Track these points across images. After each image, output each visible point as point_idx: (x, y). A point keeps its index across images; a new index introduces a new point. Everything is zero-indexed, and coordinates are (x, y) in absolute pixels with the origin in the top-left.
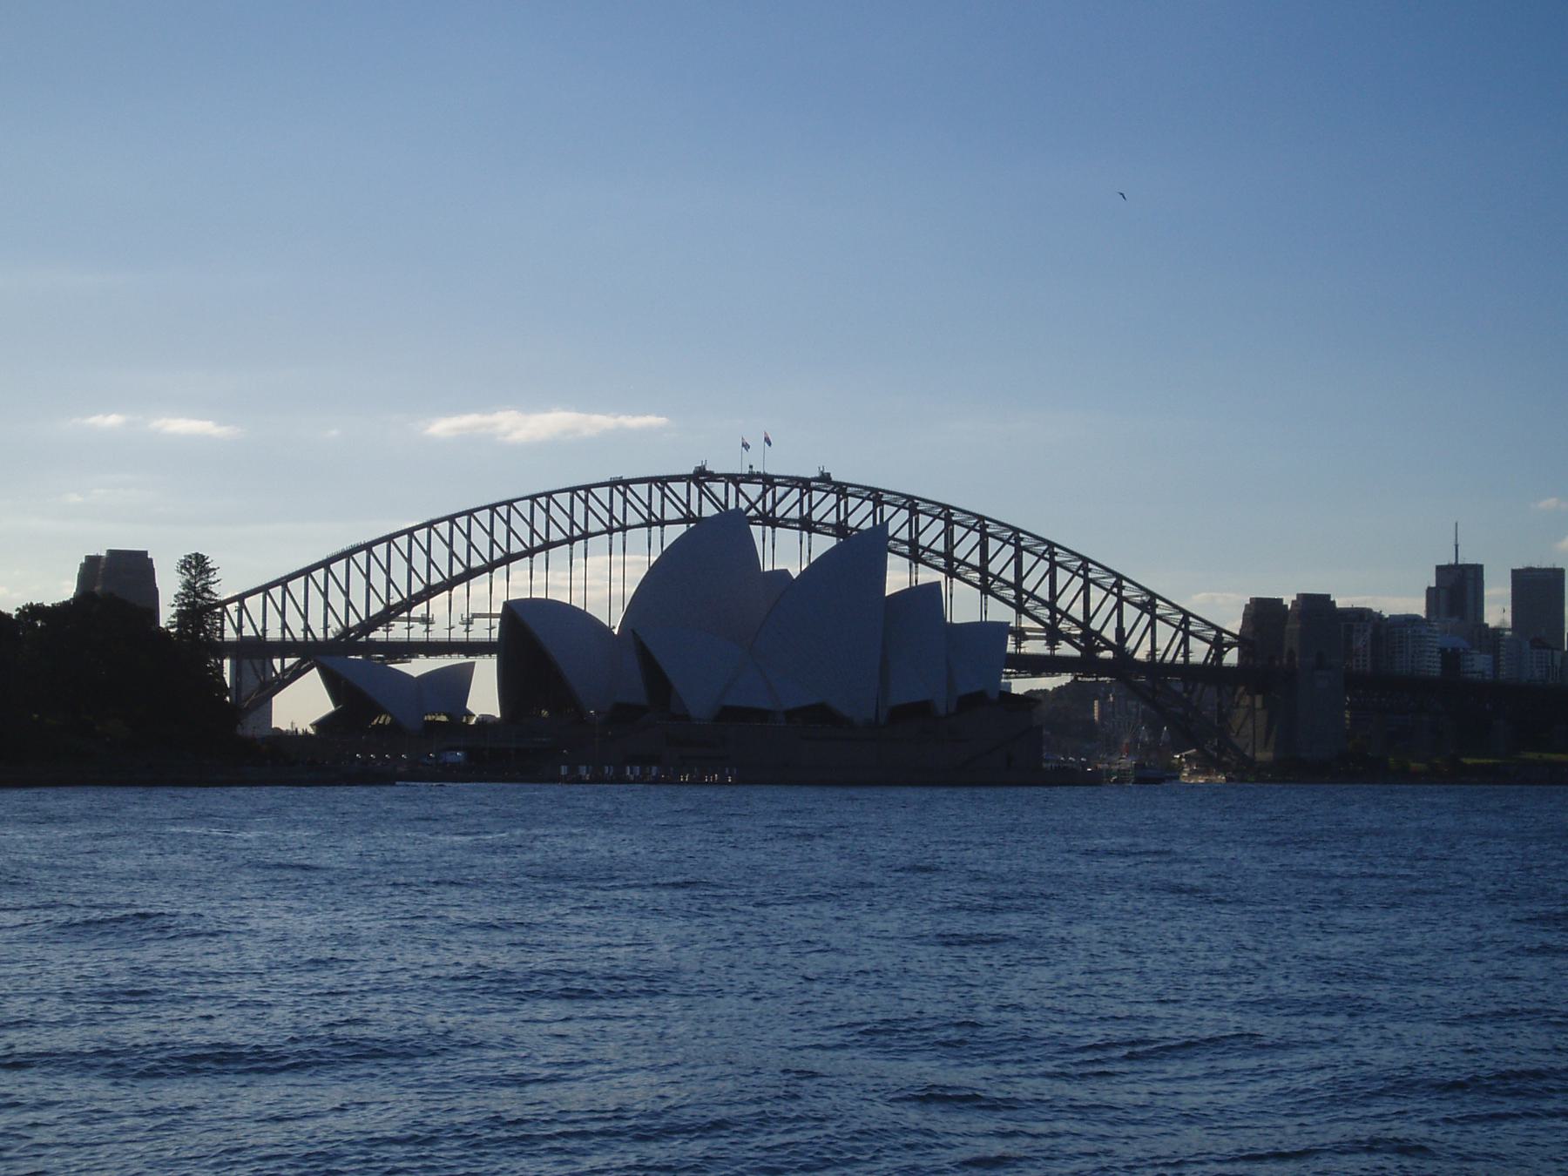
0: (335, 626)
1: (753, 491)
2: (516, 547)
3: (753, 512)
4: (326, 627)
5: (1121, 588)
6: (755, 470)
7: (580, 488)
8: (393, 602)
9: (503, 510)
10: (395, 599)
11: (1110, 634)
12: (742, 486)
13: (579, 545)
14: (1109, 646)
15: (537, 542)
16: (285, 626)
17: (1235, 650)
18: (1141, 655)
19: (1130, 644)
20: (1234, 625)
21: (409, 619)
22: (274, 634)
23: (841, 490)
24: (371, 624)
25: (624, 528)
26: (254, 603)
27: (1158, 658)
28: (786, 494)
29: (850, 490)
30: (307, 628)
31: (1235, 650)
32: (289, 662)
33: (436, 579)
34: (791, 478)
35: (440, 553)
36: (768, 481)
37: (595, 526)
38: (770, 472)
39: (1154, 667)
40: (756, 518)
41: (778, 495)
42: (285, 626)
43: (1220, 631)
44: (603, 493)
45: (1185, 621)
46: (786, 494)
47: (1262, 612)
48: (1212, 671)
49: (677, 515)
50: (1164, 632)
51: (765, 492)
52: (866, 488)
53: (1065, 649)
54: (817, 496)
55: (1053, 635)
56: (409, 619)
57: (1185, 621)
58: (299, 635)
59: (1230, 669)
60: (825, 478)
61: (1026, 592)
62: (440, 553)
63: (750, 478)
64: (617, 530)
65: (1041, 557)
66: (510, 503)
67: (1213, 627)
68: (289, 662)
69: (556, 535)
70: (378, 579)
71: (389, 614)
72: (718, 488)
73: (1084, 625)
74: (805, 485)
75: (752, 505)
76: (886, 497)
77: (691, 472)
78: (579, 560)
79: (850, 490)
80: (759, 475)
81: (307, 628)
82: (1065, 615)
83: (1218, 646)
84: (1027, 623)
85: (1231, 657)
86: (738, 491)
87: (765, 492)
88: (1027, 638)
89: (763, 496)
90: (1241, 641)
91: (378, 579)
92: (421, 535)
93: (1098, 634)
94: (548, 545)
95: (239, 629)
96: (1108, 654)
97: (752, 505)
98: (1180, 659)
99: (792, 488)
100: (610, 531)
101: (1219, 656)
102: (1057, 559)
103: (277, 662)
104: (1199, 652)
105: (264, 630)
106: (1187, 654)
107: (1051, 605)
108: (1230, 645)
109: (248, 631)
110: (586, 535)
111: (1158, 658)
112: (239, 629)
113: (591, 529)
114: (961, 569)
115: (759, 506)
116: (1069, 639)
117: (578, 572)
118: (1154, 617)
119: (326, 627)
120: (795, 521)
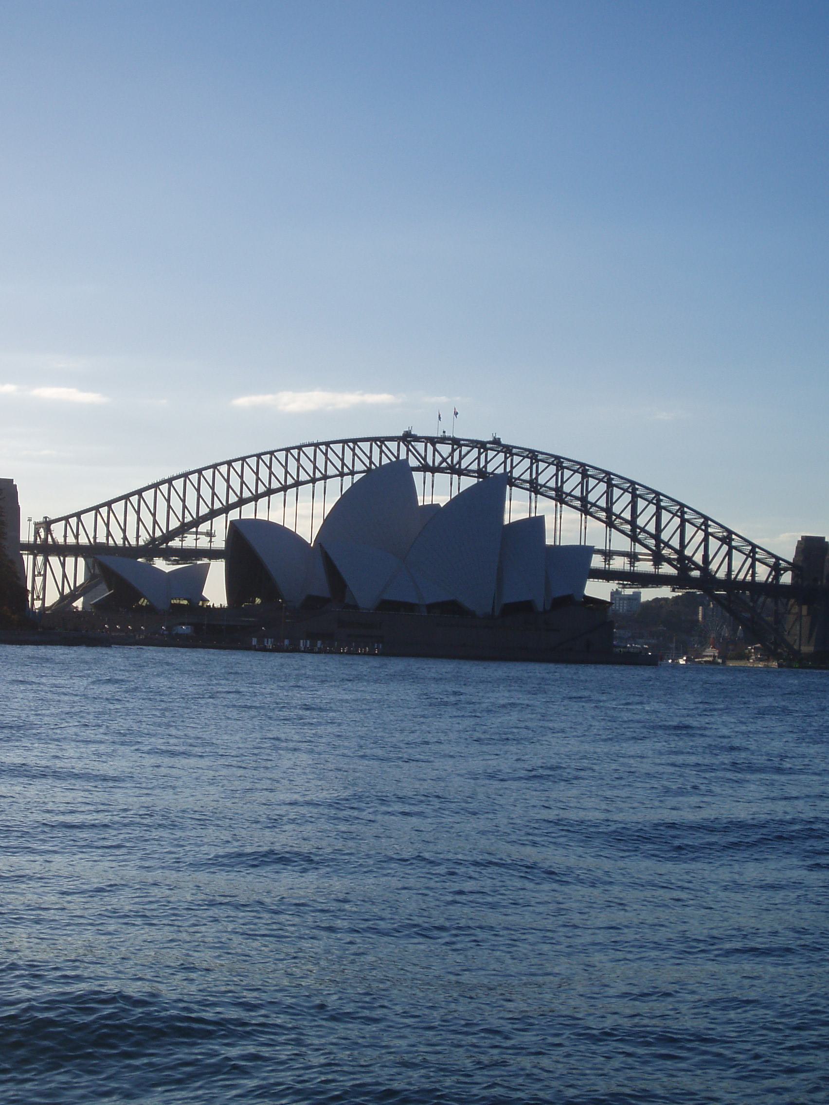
0: (144, 538)
1: (445, 449)
2: (275, 485)
3: (444, 465)
4: (138, 537)
5: (707, 526)
6: (447, 434)
7: (322, 444)
8: (186, 521)
10: (188, 519)
11: (698, 558)
12: (438, 446)
13: (320, 484)
14: (697, 567)
15: (290, 481)
16: (109, 534)
17: (789, 573)
18: (721, 575)
19: (713, 567)
20: (788, 553)
23: (508, 450)
24: (170, 535)
26: (88, 519)
27: (733, 577)
28: (469, 452)
29: (514, 451)
30: (125, 538)
31: (789, 573)
33: (217, 505)
34: (472, 441)
35: (221, 487)
36: (456, 442)
37: (331, 471)
38: (457, 436)
39: (729, 583)
40: (446, 468)
41: (463, 453)
42: (109, 534)
43: (778, 559)
44: (338, 448)
45: (753, 551)
46: (469, 452)
47: (811, 547)
48: (772, 589)
50: (738, 559)
51: (453, 450)
52: (526, 450)
53: (666, 569)
54: (491, 454)
55: (658, 558)
56: (197, 533)
57: (753, 551)
58: (120, 542)
59: (785, 586)
60: (496, 442)
61: (639, 528)
62: (221, 487)
63: (443, 440)
64: (347, 474)
65: (650, 502)
66: (271, 453)
67: (773, 556)
69: (303, 477)
71: (183, 529)
72: (420, 447)
73: (680, 552)
74: (481, 446)
75: (444, 460)
76: (540, 457)
77: (401, 434)
79: (514, 451)
80: (449, 439)
81: (125, 538)
82: (667, 545)
83: (776, 569)
84: (639, 549)
85: (786, 578)
86: (435, 450)
87: (453, 450)
88: (639, 560)
89: (451, 455)
90: (793, 567)
93: (690, 559)
94: (298, 484)
95: (77, 537)
96: (696, 573)
97: (444, 460)
98: (749, 578)
99: (473, 448)
101: (777, 577)
102: (662, 504)
104: (763, 573)
105: (95, 538)
106: (753, 575)
107: (657, 537)
108: (786, 570)
109: (83, 540)
110: (325, 477)
111: (733, 577)
112: (77, 537)
113: (329, 473)
114: (593, 509)
115: (449, 460)
116: (669, 561)
118: (731, 548)
119: (138, 537)
120: (474, 471)
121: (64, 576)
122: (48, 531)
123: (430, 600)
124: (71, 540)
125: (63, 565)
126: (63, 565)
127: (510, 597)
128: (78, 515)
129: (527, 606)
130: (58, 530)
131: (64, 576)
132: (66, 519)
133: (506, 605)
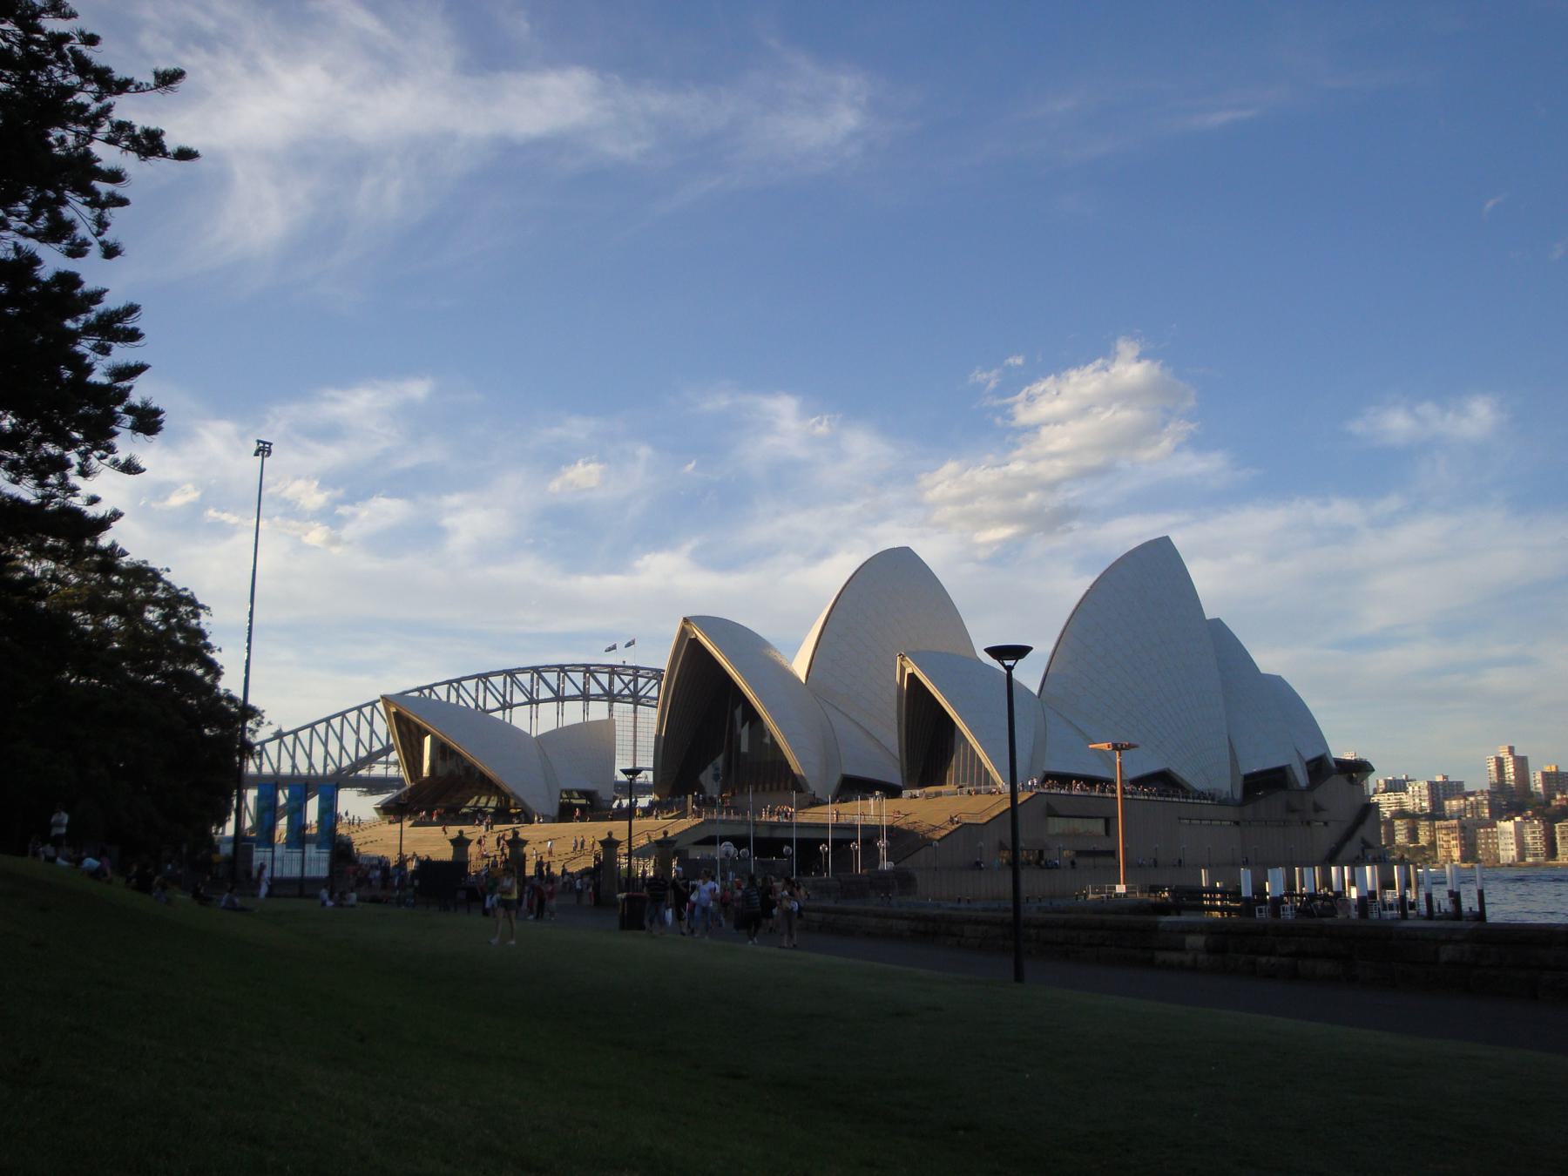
0: (331, 768)
16: (294, 766)
21: (387, 762)
22: (286, 769)
24: (359, 763)
25: (511, 706)
30: (311, 765)
42: (294, 766)
49: (550, 695)
56: (387, 762)
70: (334, 748)
71: (372, 758)
81: (311, 765)
91: (334, 748)
113: (489, 707)
119: (325, 766)
127: (1255, 764)
133: (1247, 777)
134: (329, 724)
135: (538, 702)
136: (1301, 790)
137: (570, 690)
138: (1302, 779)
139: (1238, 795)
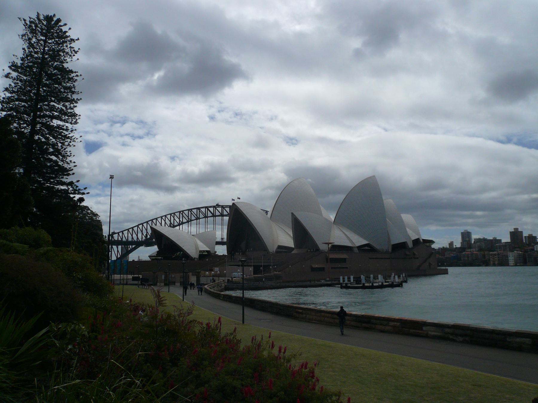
9: (173, 215)
13: (181, 226)
16: (132, 238)
22: (130, 239)
25: (199, 219)
26: (126, 233)
30: (138, 238)
32: (133, 246)
37: (193, 218)
42: (132, 238)
68: (133, 246)
69: (185, 221)
78: (190, 225)
81: (138, 238)
92: (155, 221)
94: (183, 223)
100: (197, 219)
103: (131, 246)
109: (124, 239)
110: (191, 220)
112: (122, 239)
117: (190, 227)
119: (142, 238)
121: (118, 251)
122: (113, 237)
123: (358, 244)
124: (120, 239)
125: (117, 248)
126: (117, 248)
127: (395, 241)
128: (122, 232)
129: (403, 245)
130: (116, 237)
131: (118, 251)
132: (118, 233)
133: (393, 245)
134: (143, 225)
135: (207, 217)
136: (410, 249)
137: (217, 213)
138: (410, 245)
139: (390, 250)
